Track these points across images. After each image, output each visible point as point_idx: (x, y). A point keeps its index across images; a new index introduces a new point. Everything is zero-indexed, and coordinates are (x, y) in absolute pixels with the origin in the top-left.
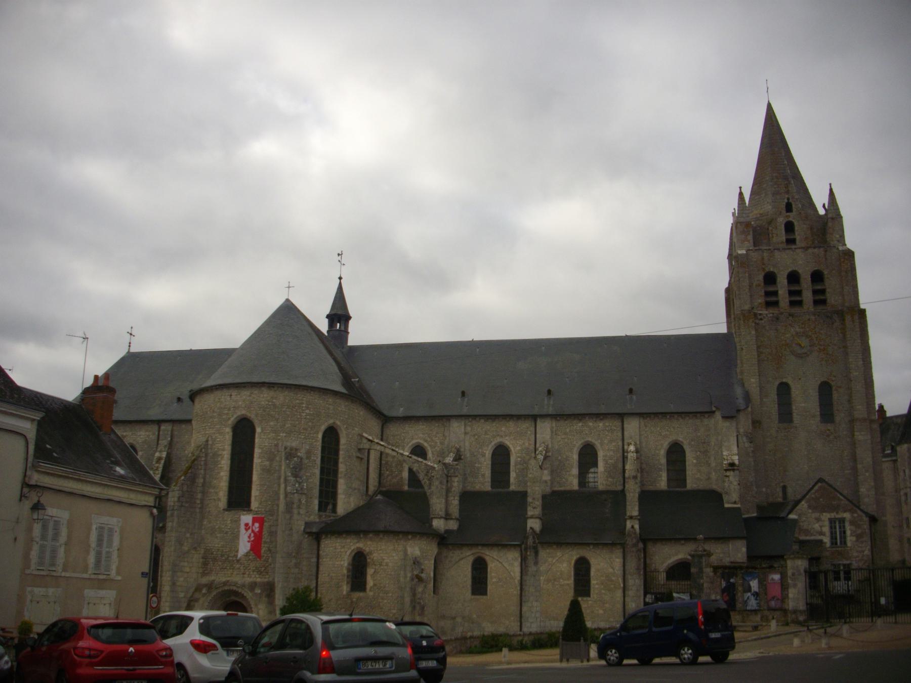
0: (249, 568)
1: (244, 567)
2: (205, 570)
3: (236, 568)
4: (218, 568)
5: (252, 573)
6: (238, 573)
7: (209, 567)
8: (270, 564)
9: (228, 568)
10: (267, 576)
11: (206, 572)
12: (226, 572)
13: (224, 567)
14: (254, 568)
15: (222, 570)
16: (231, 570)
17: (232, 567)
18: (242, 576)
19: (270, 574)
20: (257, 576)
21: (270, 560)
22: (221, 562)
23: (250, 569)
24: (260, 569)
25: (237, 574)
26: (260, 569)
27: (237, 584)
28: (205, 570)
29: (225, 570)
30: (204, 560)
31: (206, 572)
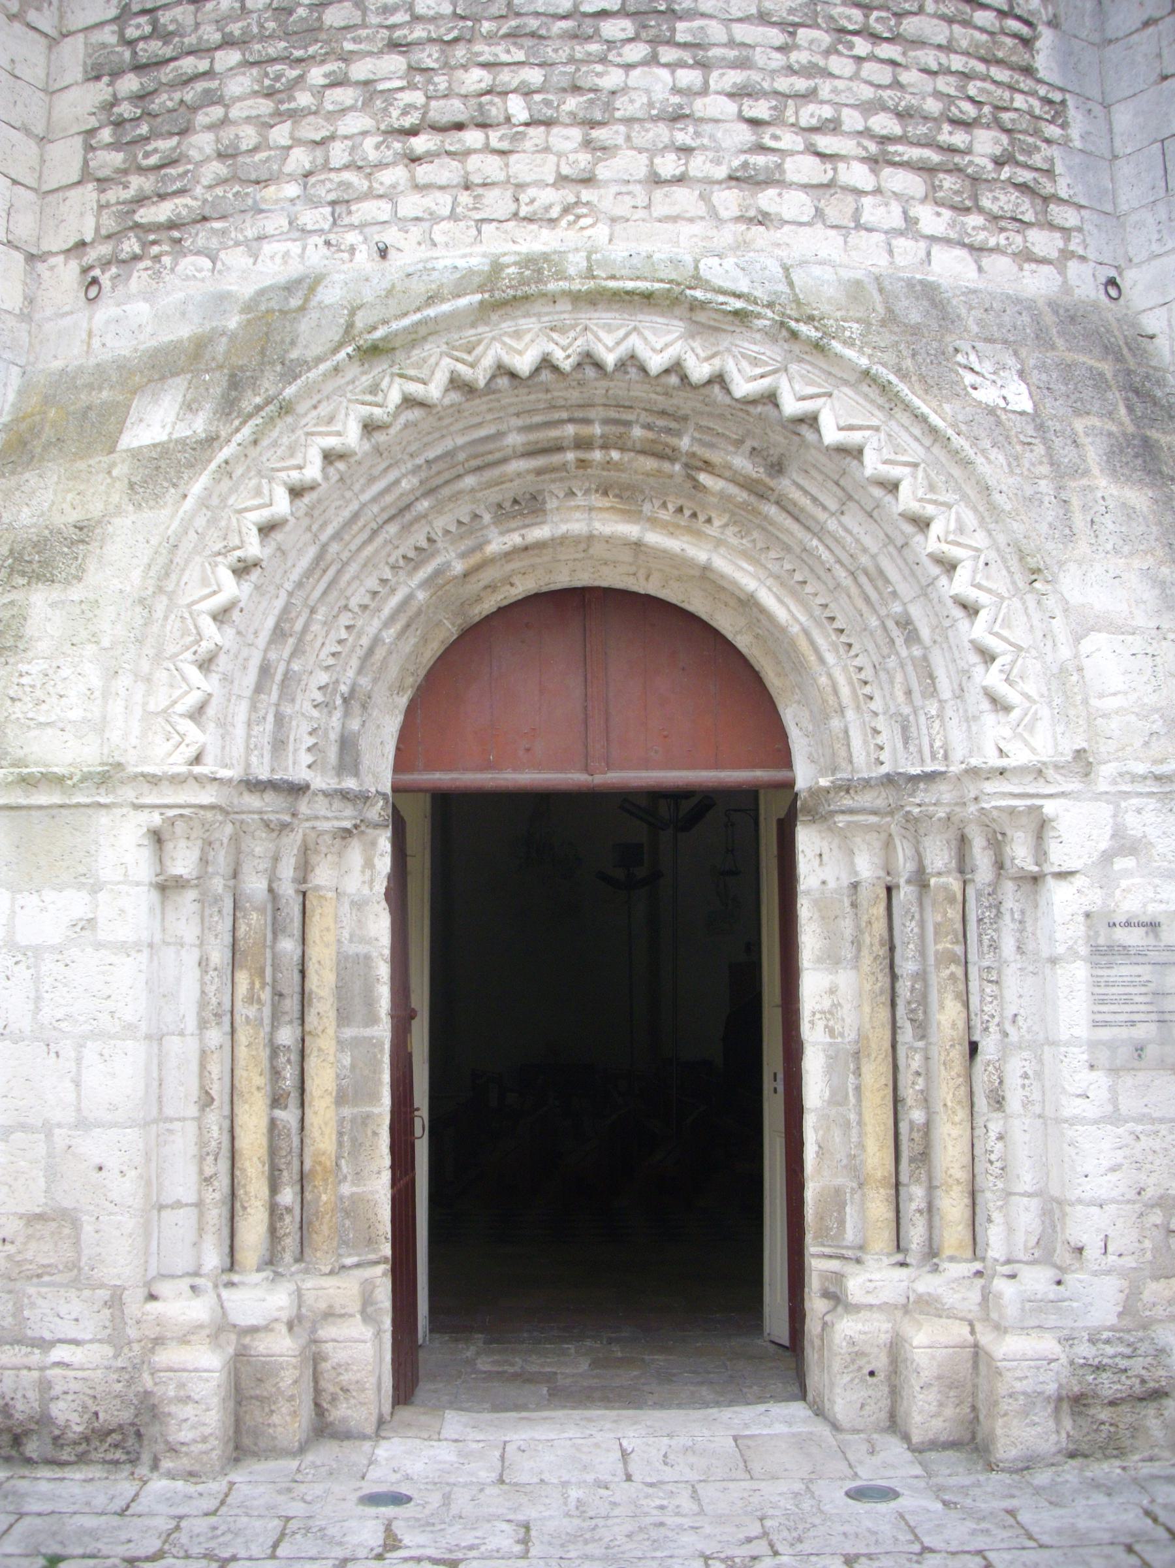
0: (809, 114)
1: (738, 94)
2: (141, 200)
3: (625, 107)
4: (353, 123)
5: (858, 175)
6: (668, 165)
7: (202, 143)
8: (1057, 111)
9: (517, 108)
10: (1043, 242)
11: (162, 212)
12: (487, 167)
13: (455, 109)
14: (884, 123)
15: (421, 143)
16: (567, 138)
17: (572, 103)
18: (729, 200)
19: (1068, 217)
20: (933, 220)
21: (1044, 60)
22: (395, 46)
23: (832, 126)
24: (959, 138)
25: (656, 180)
26: (959, 138)
27: (698, 281)
28: (141, 200)
29: (473, 138)
30: (130, 83)
31: (162, 212)
